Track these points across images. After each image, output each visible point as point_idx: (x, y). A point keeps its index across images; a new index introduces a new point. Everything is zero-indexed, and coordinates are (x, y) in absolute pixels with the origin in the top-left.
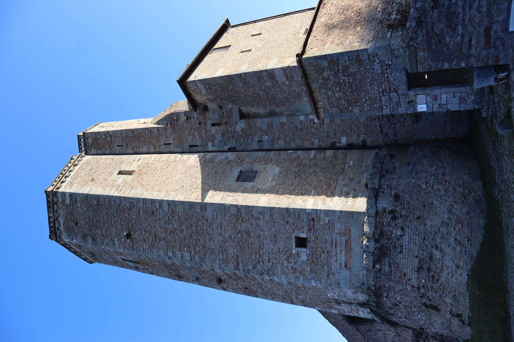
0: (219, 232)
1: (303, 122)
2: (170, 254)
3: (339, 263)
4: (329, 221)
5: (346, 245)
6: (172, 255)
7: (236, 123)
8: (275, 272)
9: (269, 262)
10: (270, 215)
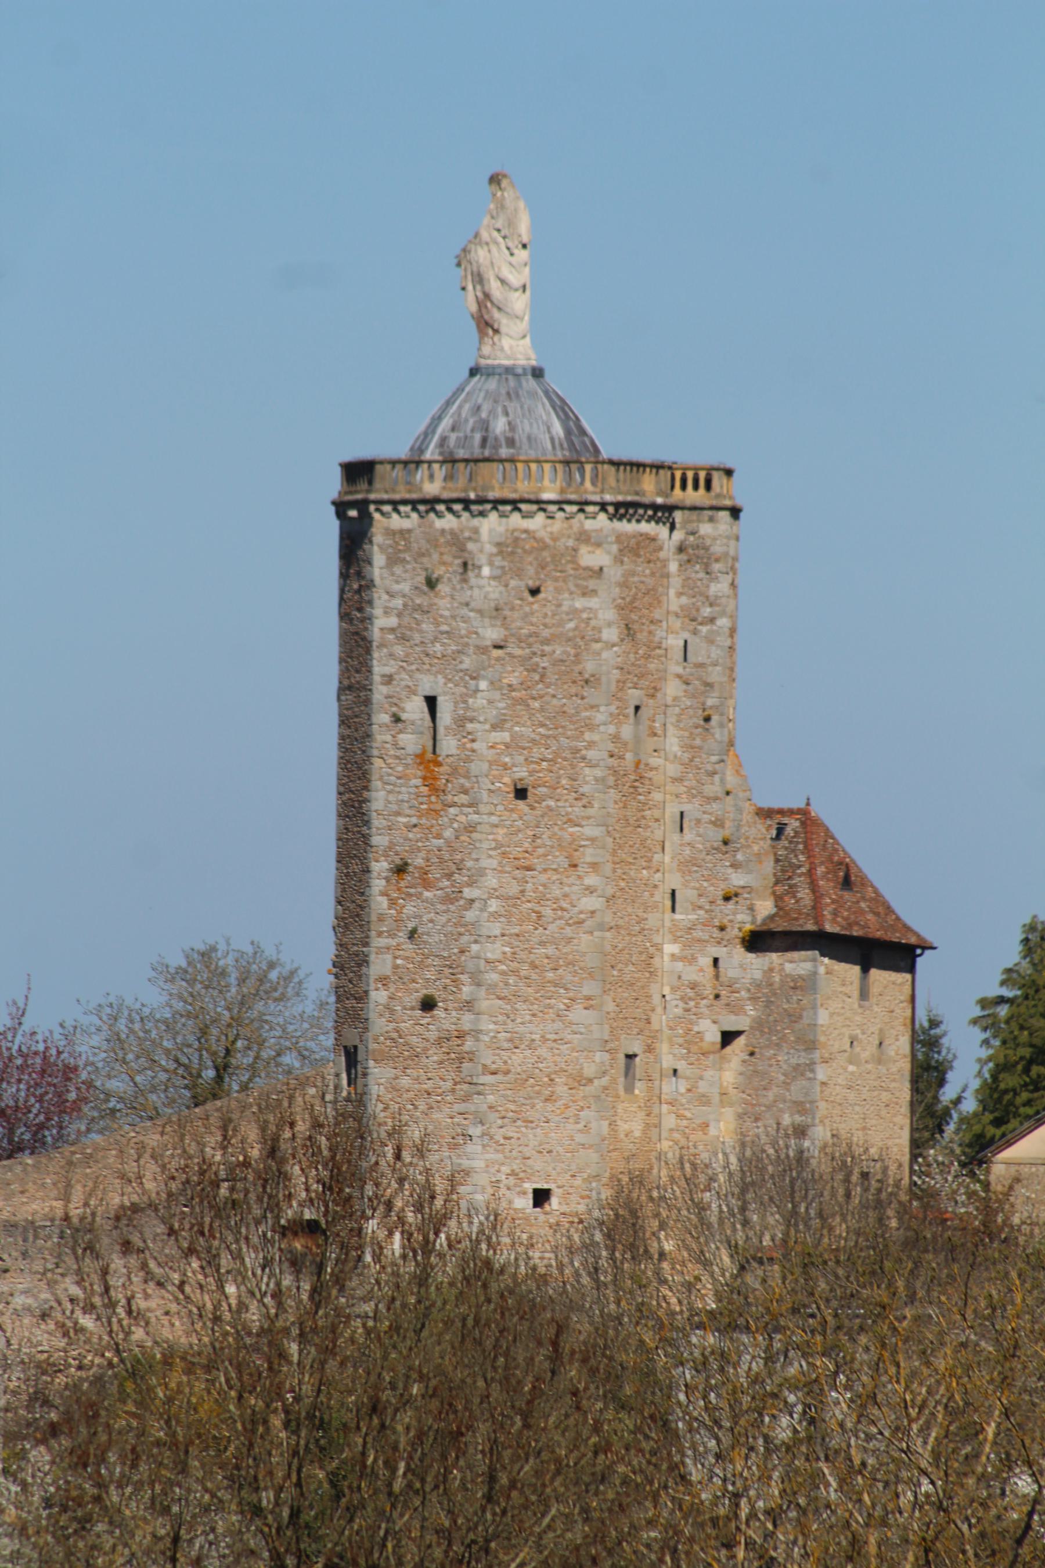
6: (491, 910)
7: (715, 1022)
9: (505, 1138)
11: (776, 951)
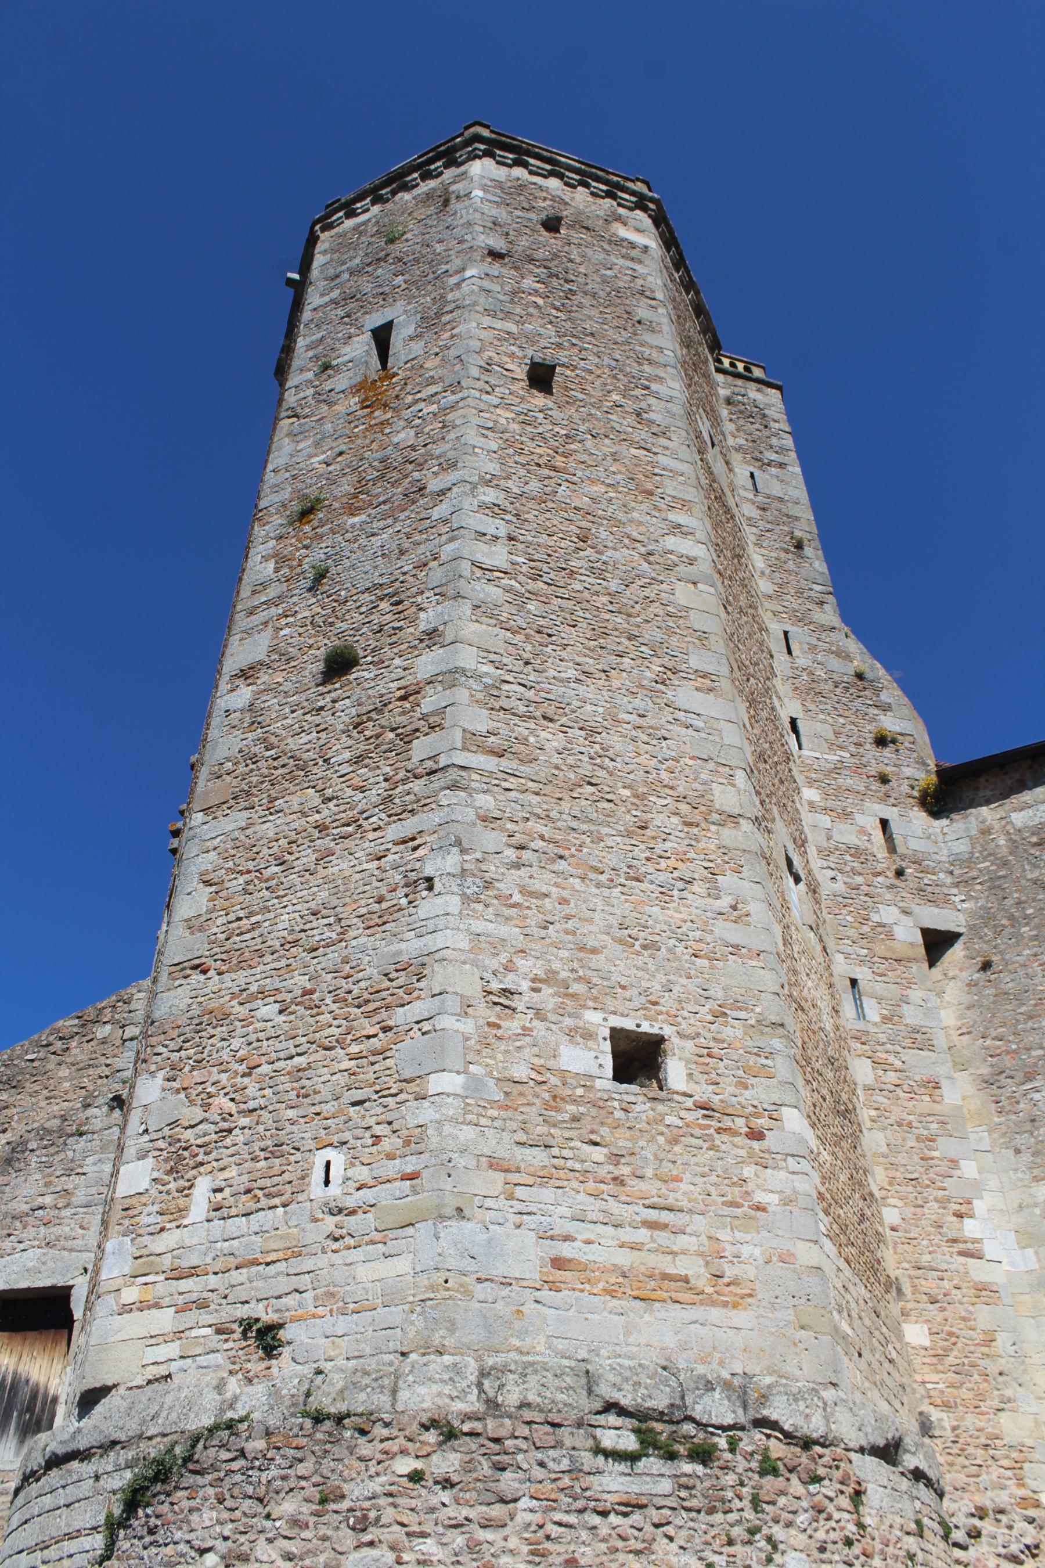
0: (623, 716)
1: (958, 1173)
3: (571, 1228)
4: (760, 1208)
5: (666, 1277)
7: (906, 912)
8: (480, 907)
10: (737, 947)
11: (987, 802)
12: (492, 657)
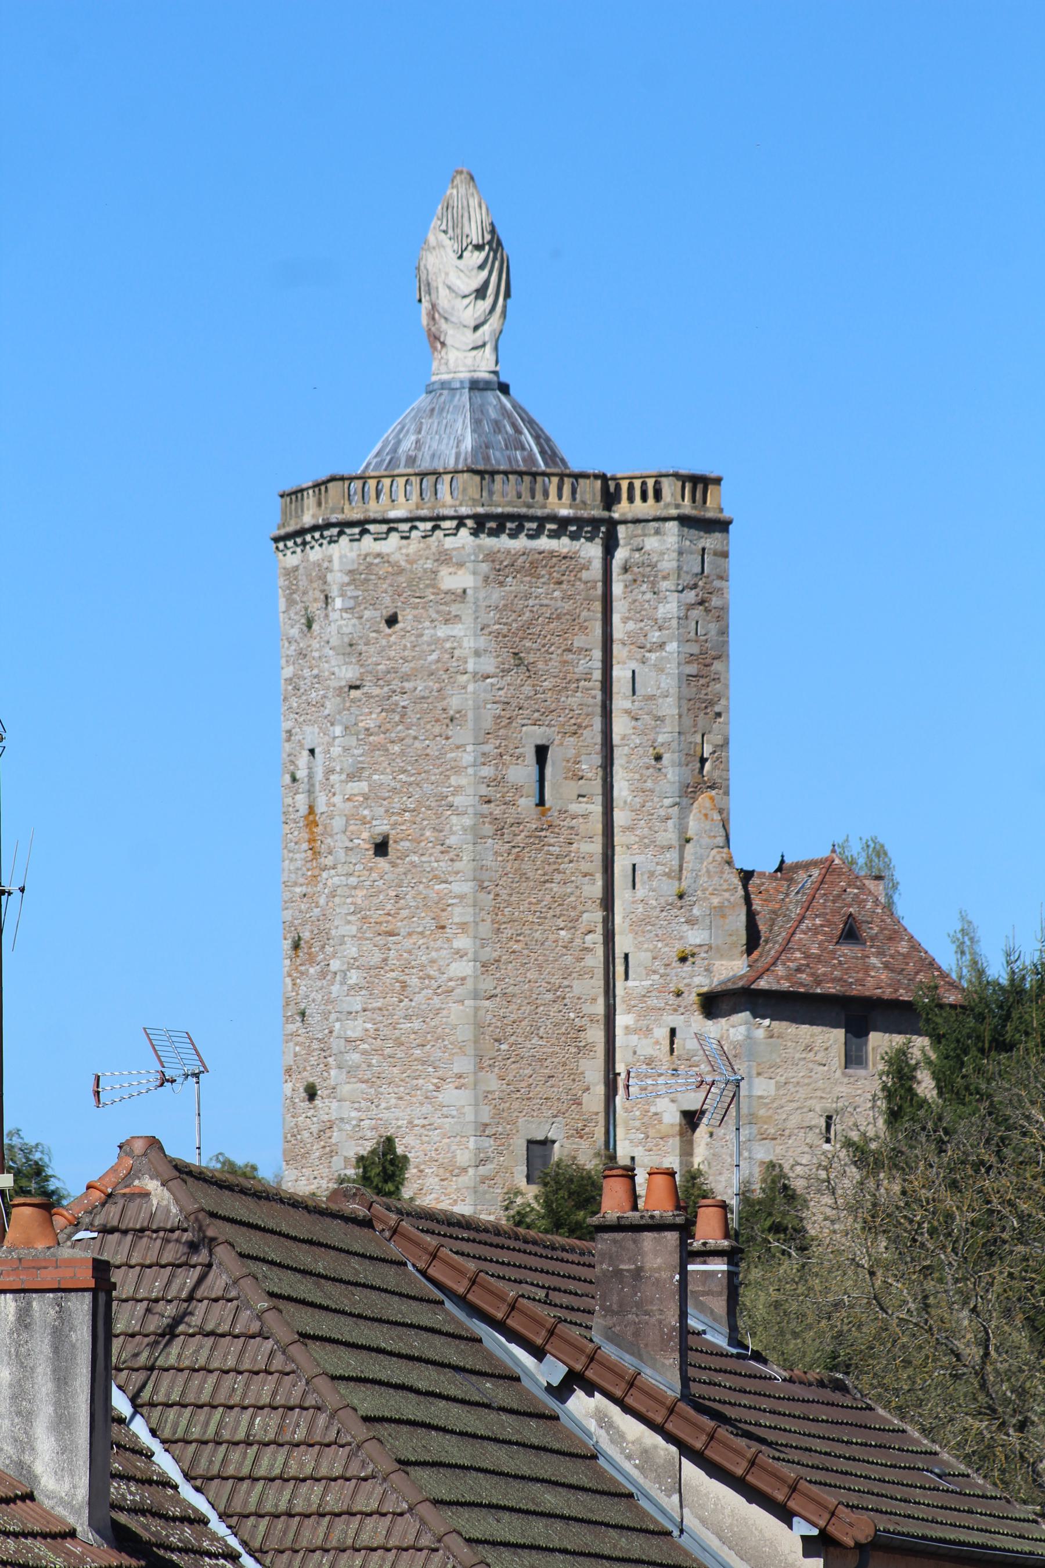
2: (354, 977)
7: (673, 1101)
12: (356, 1105)
